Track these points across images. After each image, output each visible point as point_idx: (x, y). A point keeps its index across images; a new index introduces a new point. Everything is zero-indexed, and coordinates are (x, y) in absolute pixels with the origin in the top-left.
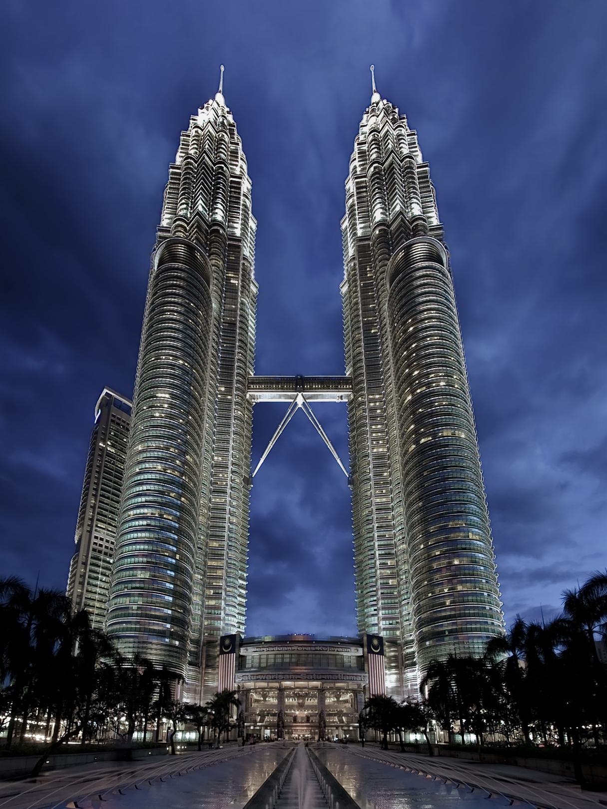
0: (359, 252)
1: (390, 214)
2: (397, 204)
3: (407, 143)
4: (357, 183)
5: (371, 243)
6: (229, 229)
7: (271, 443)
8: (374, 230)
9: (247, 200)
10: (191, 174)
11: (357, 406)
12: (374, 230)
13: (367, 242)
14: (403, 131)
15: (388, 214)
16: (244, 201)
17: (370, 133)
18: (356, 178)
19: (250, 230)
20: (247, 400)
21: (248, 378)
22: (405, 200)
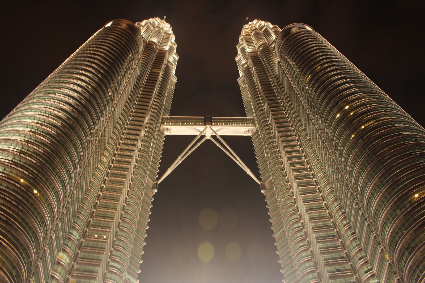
7: (180, 158)
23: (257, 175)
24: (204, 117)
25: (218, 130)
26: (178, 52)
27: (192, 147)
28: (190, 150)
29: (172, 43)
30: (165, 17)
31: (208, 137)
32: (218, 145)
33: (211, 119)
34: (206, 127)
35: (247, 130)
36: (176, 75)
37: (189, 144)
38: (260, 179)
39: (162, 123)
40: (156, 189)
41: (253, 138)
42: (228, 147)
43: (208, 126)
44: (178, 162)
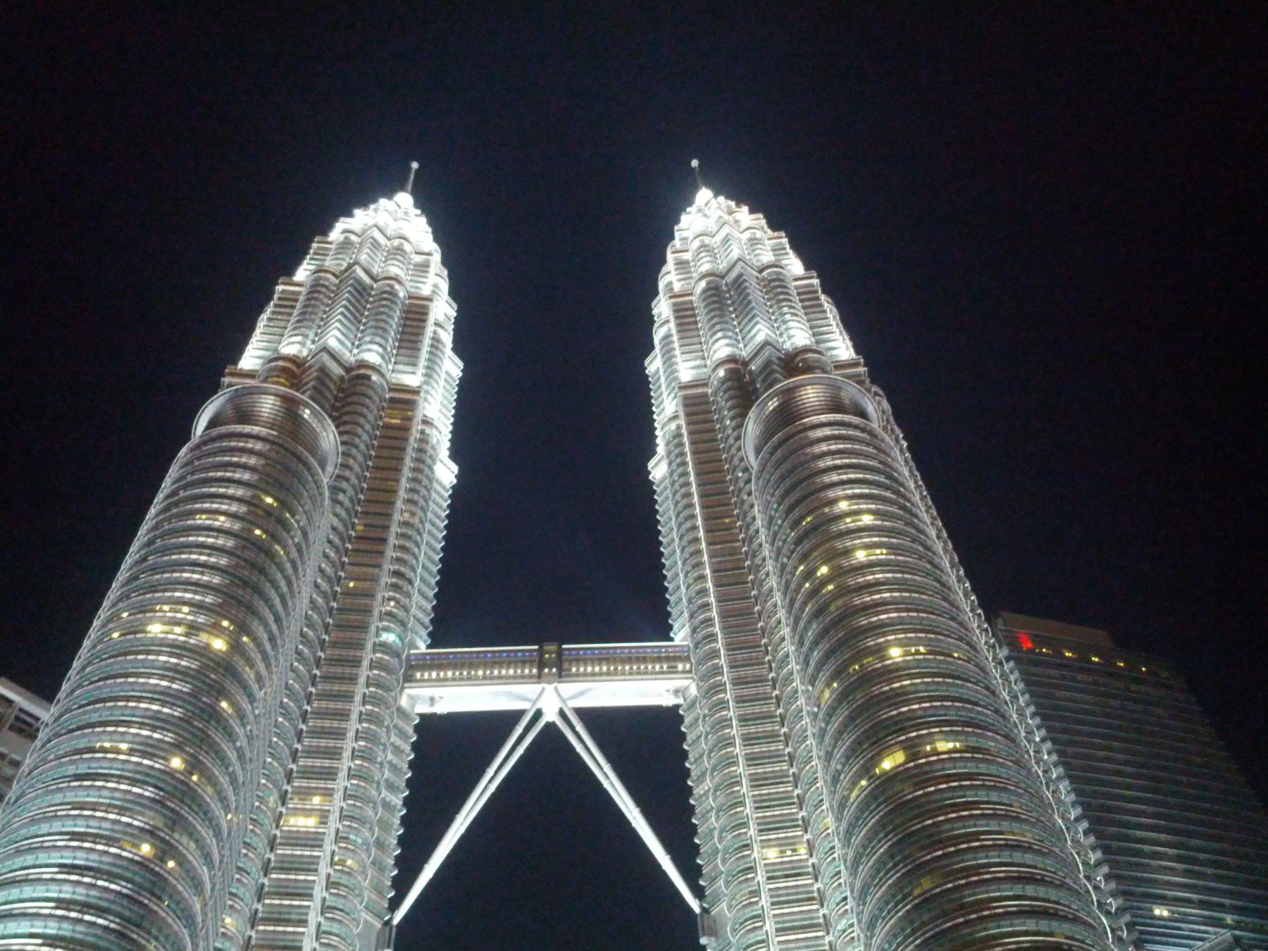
0: (685, 406)
1: (745, 346)
2: (759, 331)
3: (769, 248)
4: (675, 304)
5: (710, 391)
6: (393, 375)
8: (714, 369)
9: (440, 331)
10: (324, 293)
11: (706, 711)
12: (714, 369)
13: (700, 390)
14: (759, 234)
15: (741, 345)
16: (435, 332)
17: (696, 237)
18: (671, 297)
19: (443, 376)
20: (401, 711)
21: (409, 655)
22: (775, 325)
23: (691, 873)
24: (536, 647)
25: (581, 694)
26: (458, 348)
27: (496, 773)
28: (490, 781)
29: (437, 324)
30: (415, 165)
31: (550, 716)
32: (579, 749)
33: (560, 653)
34: (543, 689)
35: (672, 689)
36: (455, 455)
37: (488, 764)
38: (699, 892)
39: (409, 679)
40: (389, 947)
41: (687, 721)
42: (607, 768)
43: (549, 688)
44: (458, 829)
